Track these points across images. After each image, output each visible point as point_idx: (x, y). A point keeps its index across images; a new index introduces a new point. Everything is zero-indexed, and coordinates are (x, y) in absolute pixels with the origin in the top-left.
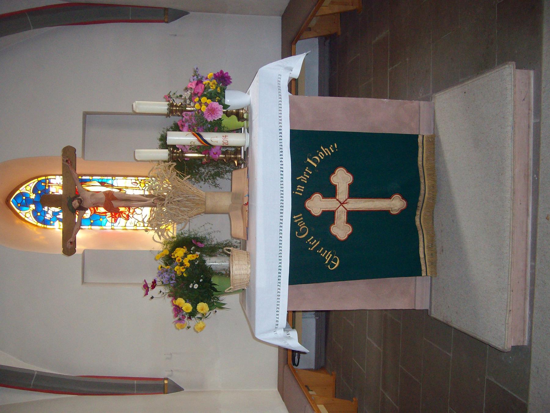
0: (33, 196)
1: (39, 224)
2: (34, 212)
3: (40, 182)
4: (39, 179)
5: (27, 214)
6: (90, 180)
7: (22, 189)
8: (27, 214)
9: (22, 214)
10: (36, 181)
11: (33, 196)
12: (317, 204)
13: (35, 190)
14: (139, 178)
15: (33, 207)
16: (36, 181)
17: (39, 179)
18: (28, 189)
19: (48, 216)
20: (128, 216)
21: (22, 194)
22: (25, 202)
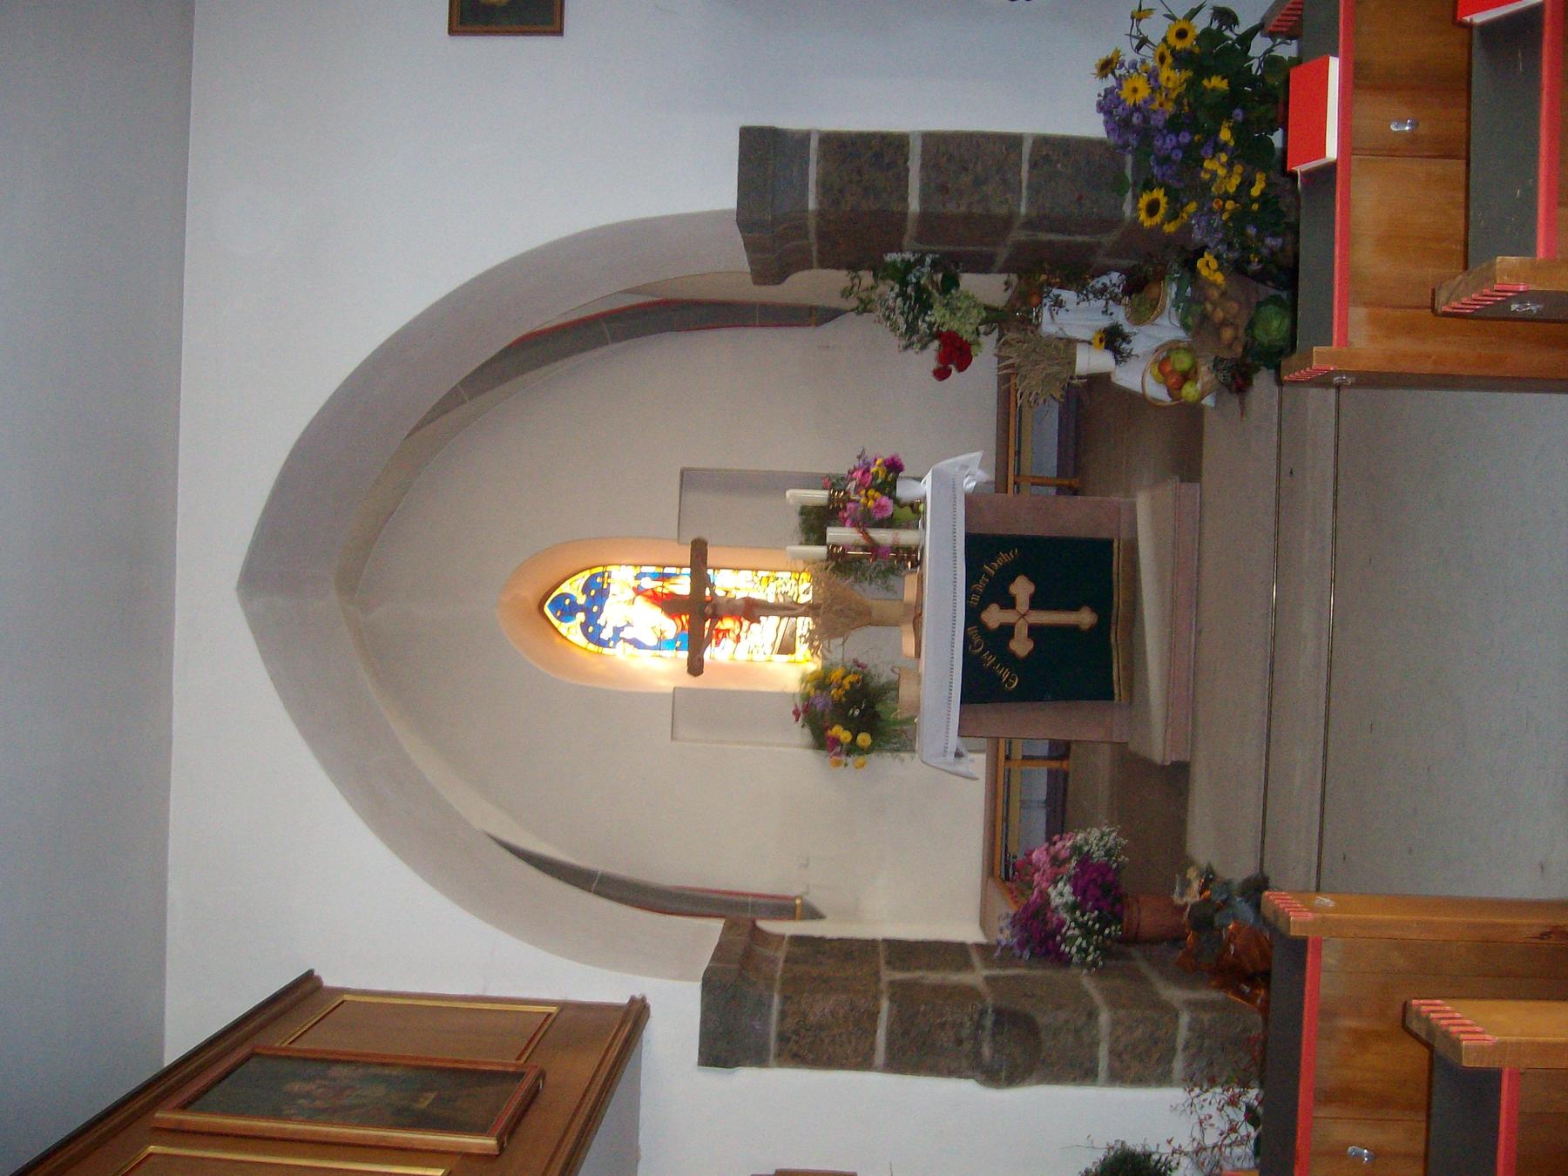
0: (581, 600)
1: (592, 647)
2: (584, 626)
3: (594, 577)
4: (595, 571)
5: (572, 630)
6: (676, 575)
7: (565, 588)
8: (572, 630)
9: (562, 627)
10: (587, 574)
11: (581, 600)
12: (994, 617)
13: (586, 590)
14: (761, 573)
15: (581, 617)
16: (587, 574)
17: (595, 571)
18: (573, 588)
19: (606, 634)
20: (738, 637)
21: (566, 596)
22: (566, 609)
